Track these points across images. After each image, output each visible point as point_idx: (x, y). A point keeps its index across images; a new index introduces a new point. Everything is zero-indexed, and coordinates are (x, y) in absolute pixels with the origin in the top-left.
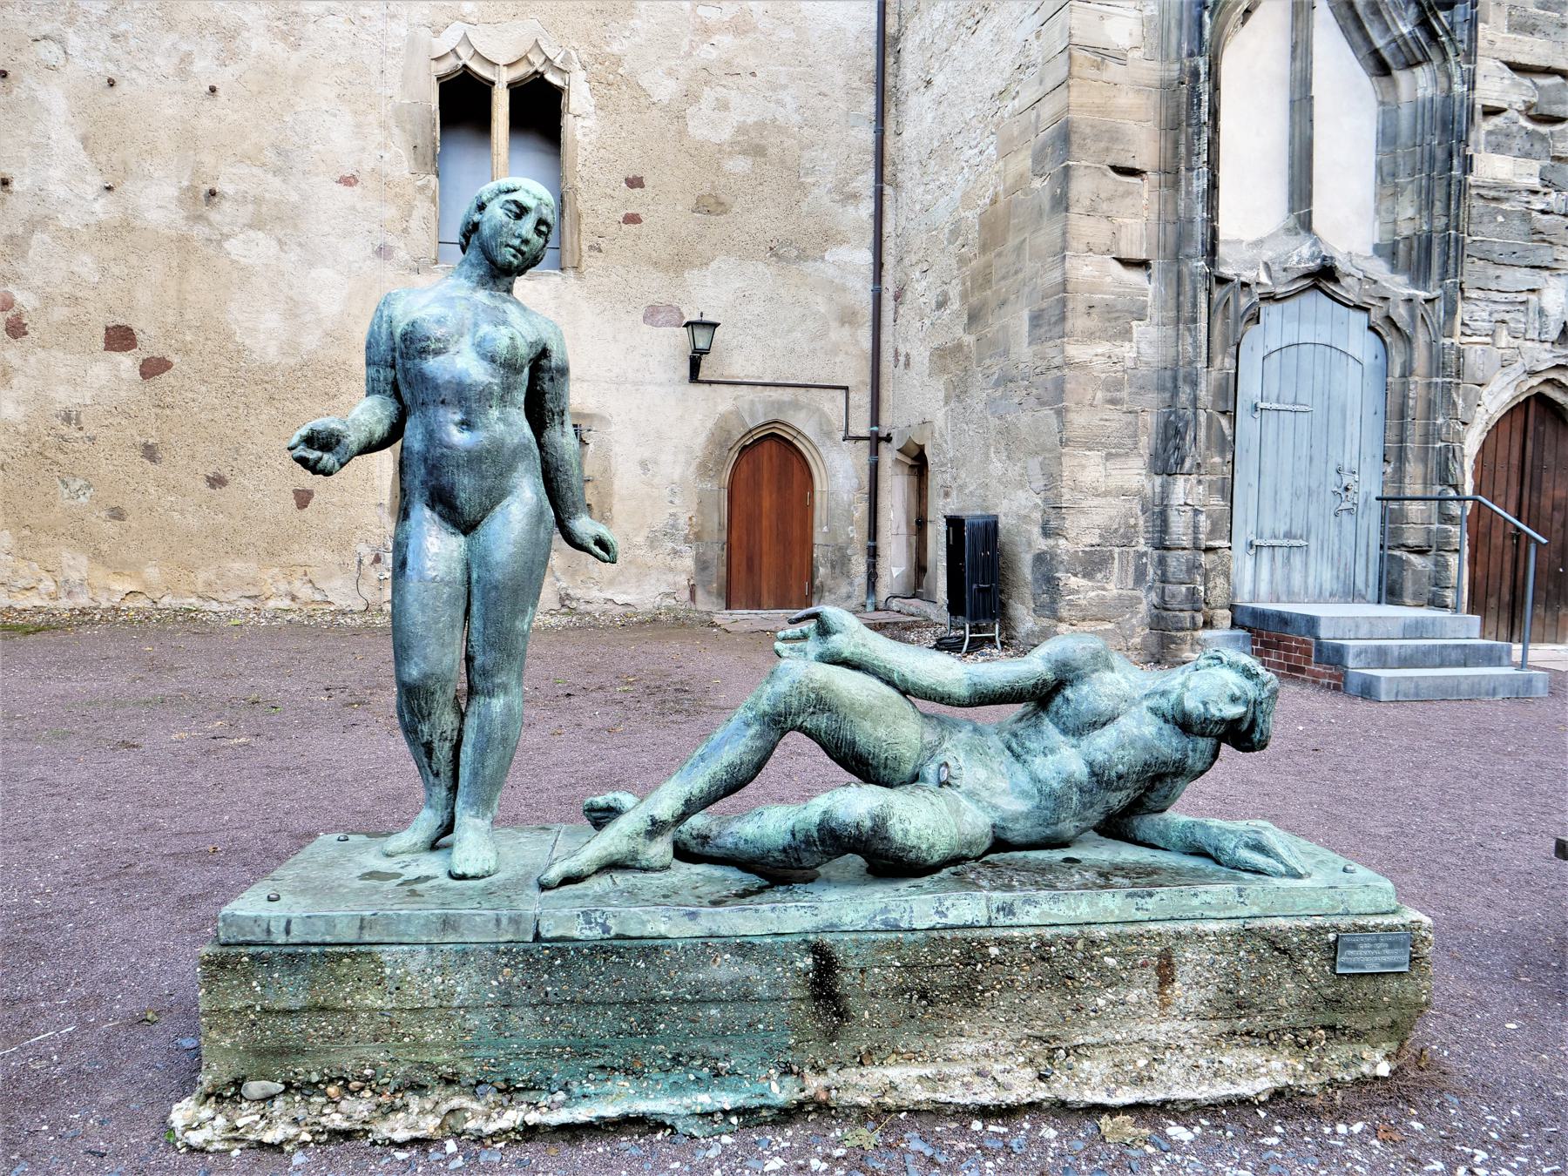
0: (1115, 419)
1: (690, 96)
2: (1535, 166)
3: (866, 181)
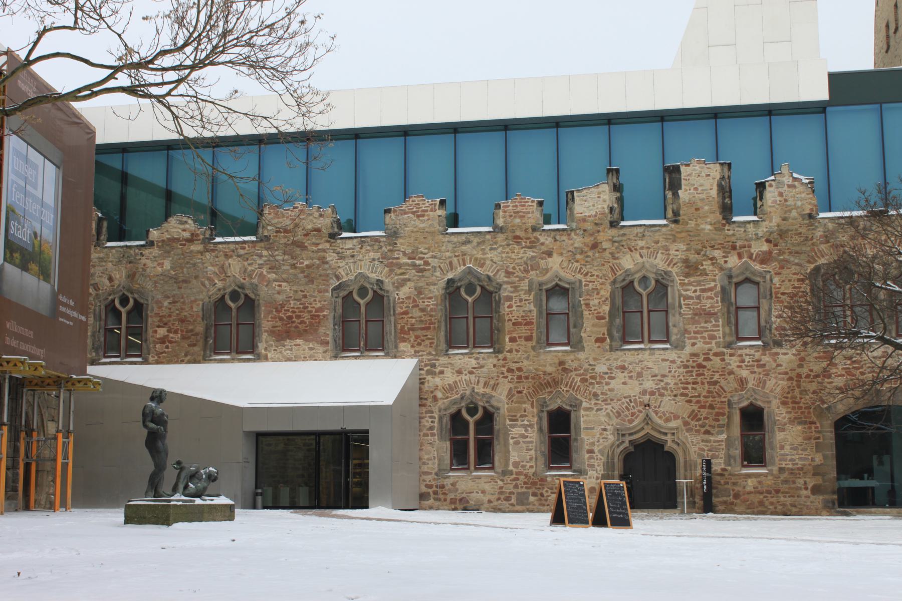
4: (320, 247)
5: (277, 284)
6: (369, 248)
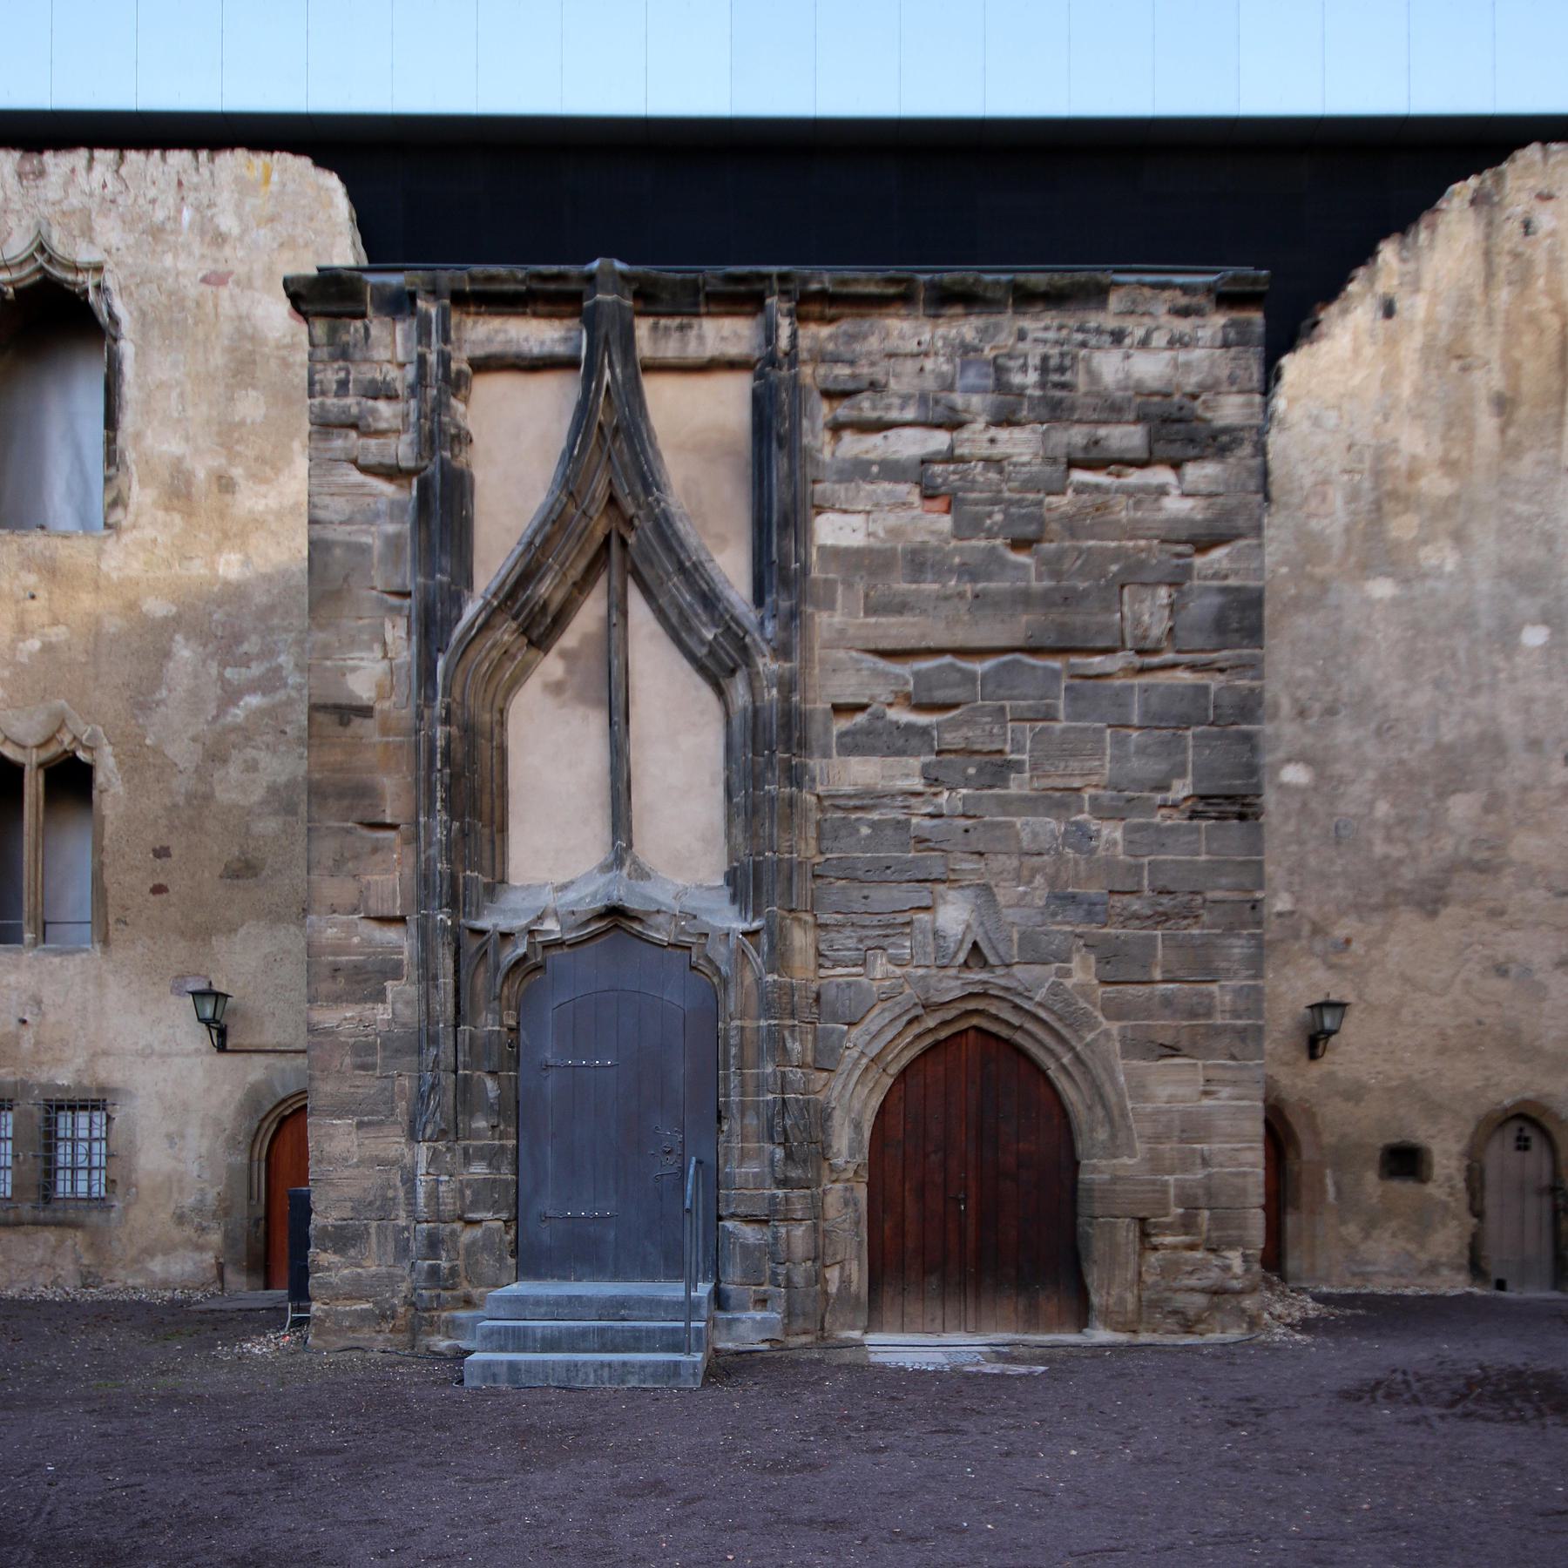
0: (367, 1085)
2: (915, 763)
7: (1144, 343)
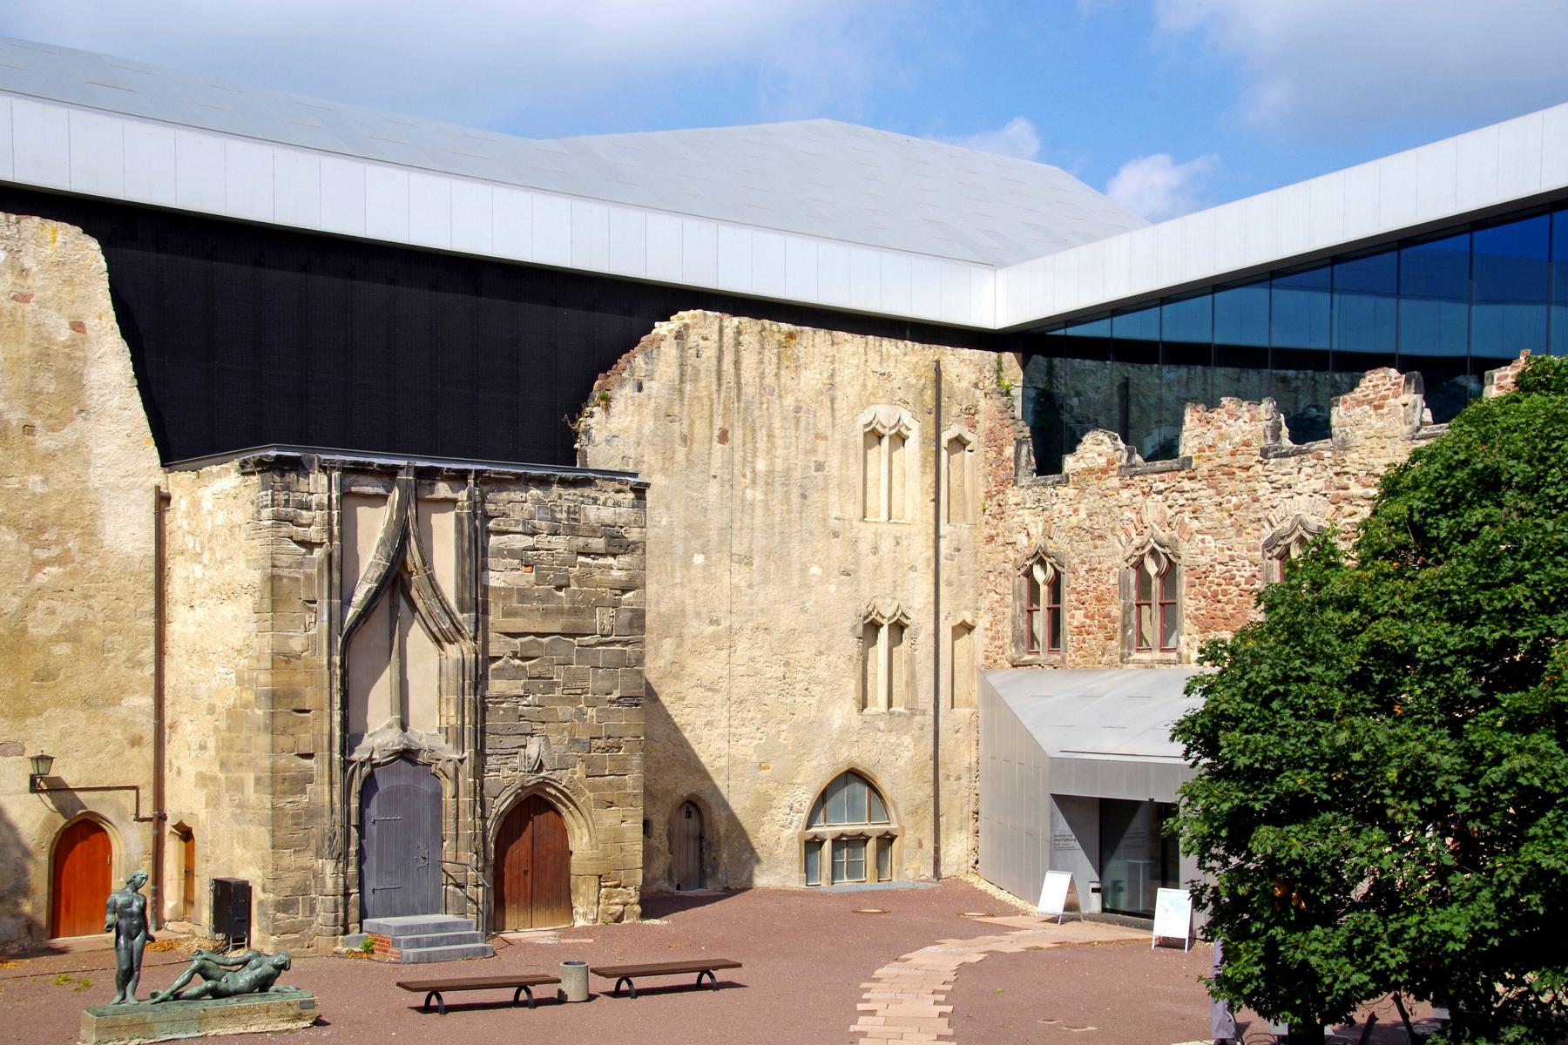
1: (27, 607)
3: (149, 653)
4: (1250, 473)
5: (1200, 537)
6: (1310, 471)
7: (604, 504)
